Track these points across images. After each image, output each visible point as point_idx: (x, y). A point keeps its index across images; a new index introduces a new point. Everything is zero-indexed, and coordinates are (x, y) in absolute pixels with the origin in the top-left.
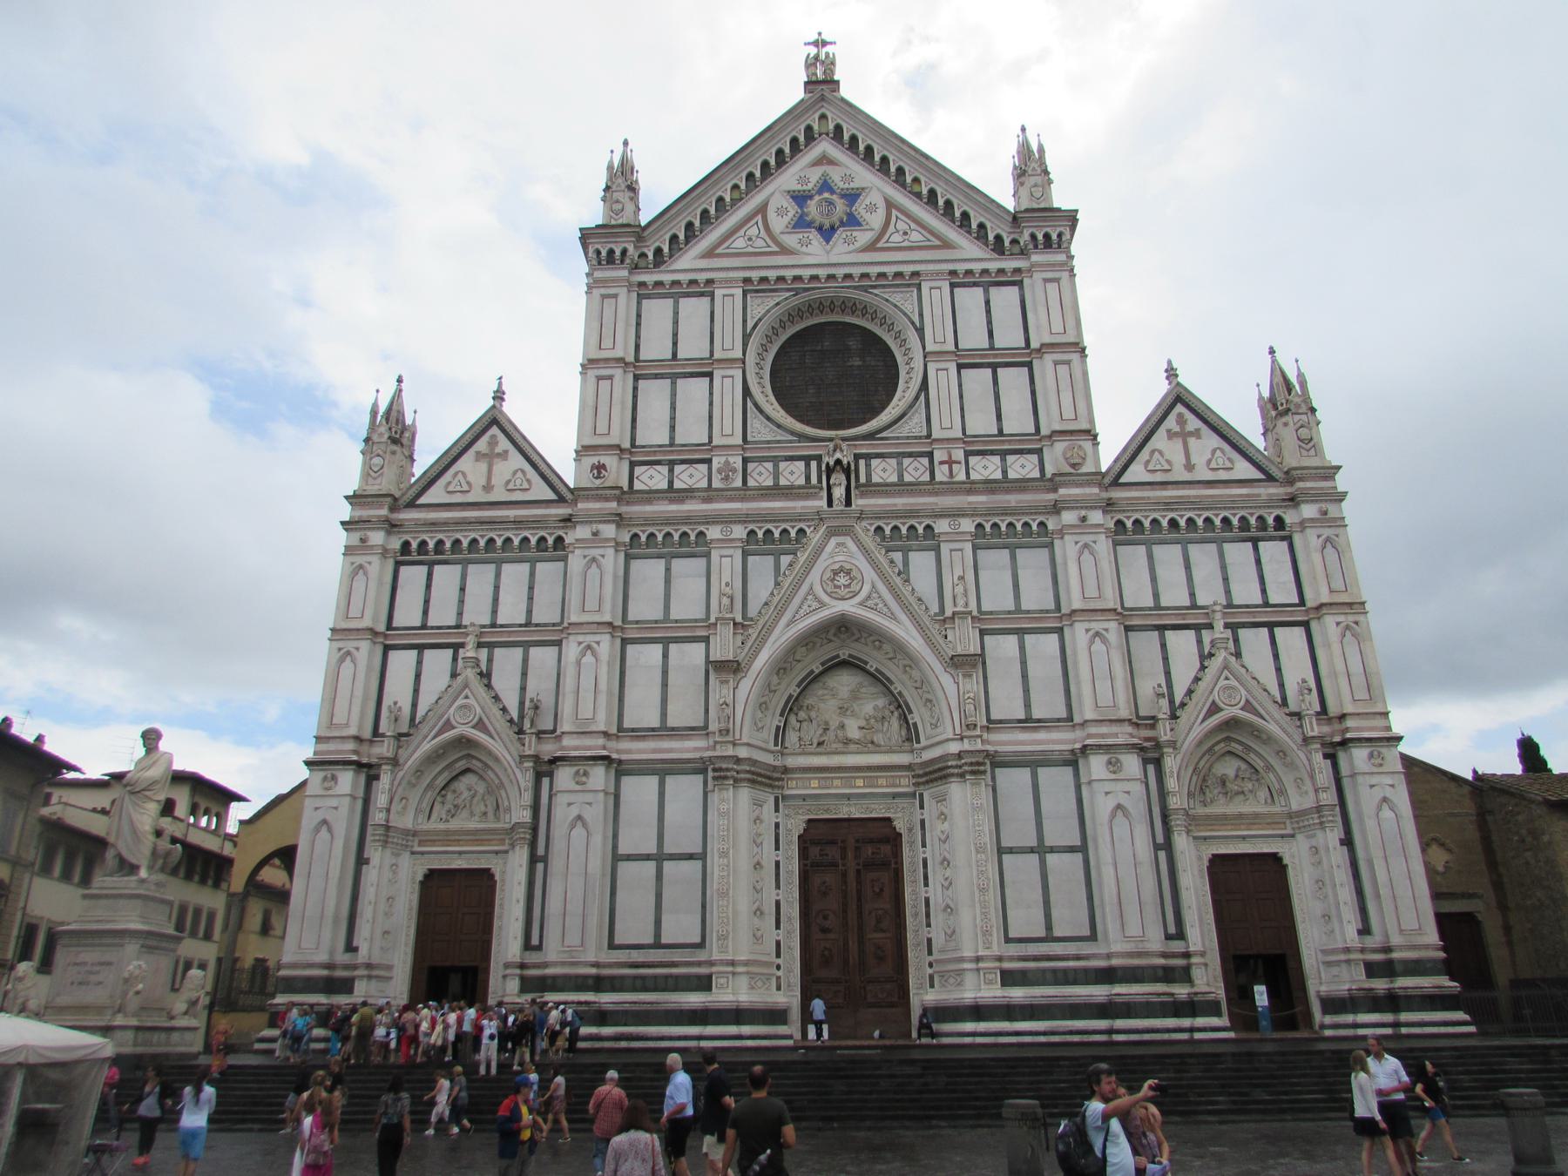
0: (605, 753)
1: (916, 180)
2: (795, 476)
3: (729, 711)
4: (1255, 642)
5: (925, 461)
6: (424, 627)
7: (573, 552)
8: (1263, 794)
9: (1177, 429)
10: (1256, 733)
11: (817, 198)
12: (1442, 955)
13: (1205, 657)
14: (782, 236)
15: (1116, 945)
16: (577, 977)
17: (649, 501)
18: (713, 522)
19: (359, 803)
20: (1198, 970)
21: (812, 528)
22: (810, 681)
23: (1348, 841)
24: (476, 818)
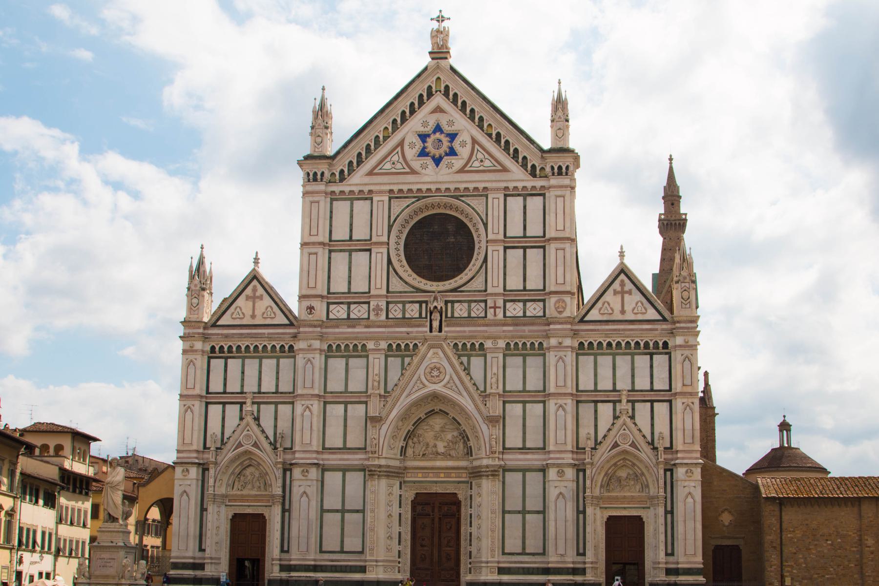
0: (316, 461)
1: (490, 125)
2: (414, 312)
5: (483, 305)
6: (225, 392)
7: (298, 354)
8: (638, 487)
9: (619, 289)
10: (638, 458)
11: (433, 137)
12: (702, 566)
13: (616, 417)
15: (553, 560)
16: (305, 565)
19: (200, 482)
22: (419, 422)
23: (670, 512)
24: (256, 489)
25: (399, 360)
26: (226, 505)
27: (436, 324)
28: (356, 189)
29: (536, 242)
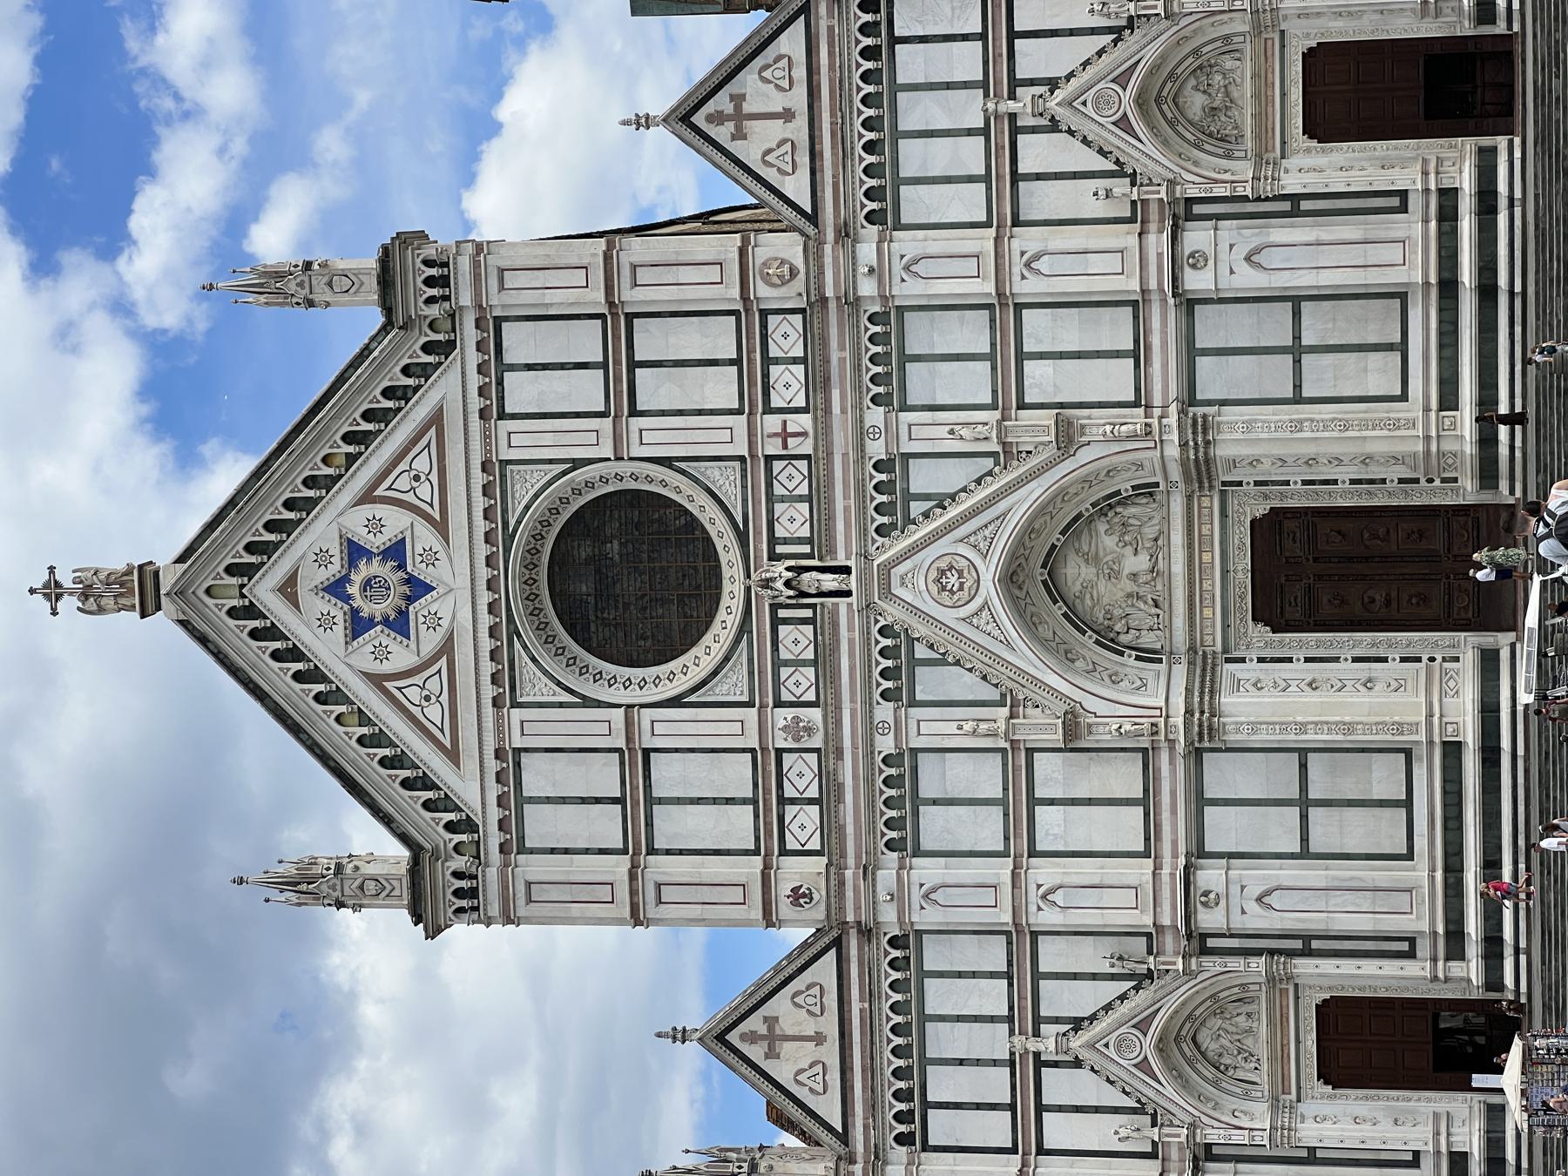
0: (1180, 872)
1: (326, 460)
3: (1127, 727)
4: (1033, 59)
6: (1012, 1107)
7: (912, 924)
8: (1229, 63)
9: (730, 126)
11: (358, 602)
13: (1054, 126)
14: (421, 655)
16: (1446, 896)
17: (841, 829)
18: (871, 746)
19: (1241, 1166)
20: (1444, 181)
21: (879, 618)
24: (1255, 1025)
25: (920, 671)
26: (1299, 1100)
27: (830, 582)
28: (493, 791)
29: (616, 337)
